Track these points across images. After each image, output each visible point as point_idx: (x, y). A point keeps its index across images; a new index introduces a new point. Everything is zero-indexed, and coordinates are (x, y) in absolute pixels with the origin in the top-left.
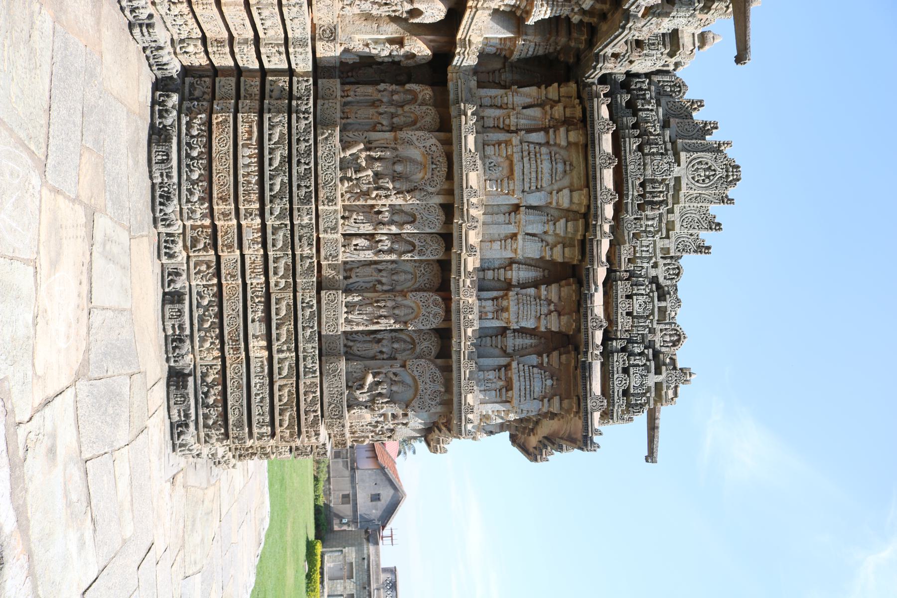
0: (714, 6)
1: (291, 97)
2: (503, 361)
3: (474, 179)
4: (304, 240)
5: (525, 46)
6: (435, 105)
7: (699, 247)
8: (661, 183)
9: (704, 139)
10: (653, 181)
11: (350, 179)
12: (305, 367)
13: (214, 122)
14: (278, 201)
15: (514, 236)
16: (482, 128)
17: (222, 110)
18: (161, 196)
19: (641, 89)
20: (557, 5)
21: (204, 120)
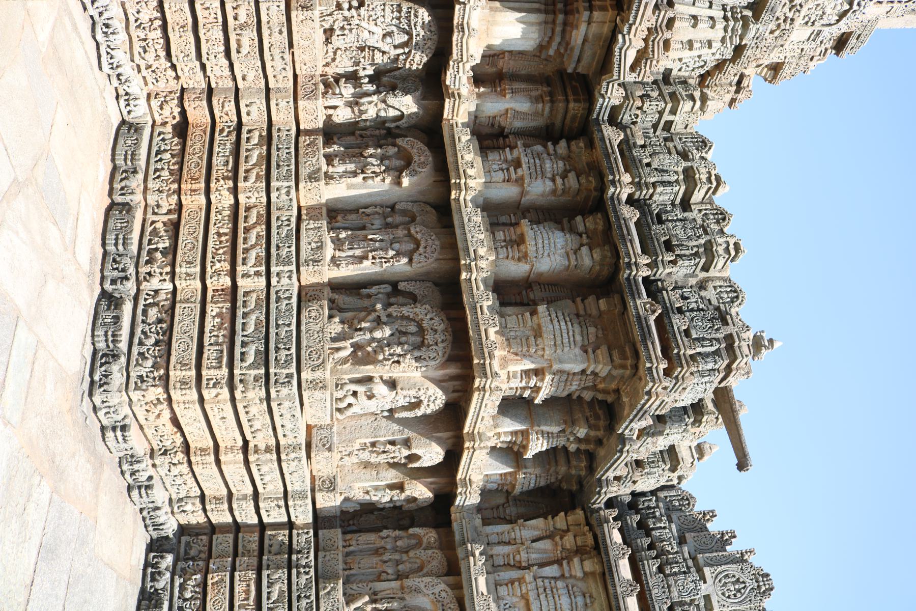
0: (704, 419)
1: (290, 551)
5: (526, 480)
6: (441, 548)
9: (725, 551)
13: (210, 582)
16: (493, 568)
17: (218, 570)
19: (649, 508)
20: (553, 437)
21: (199, 581)
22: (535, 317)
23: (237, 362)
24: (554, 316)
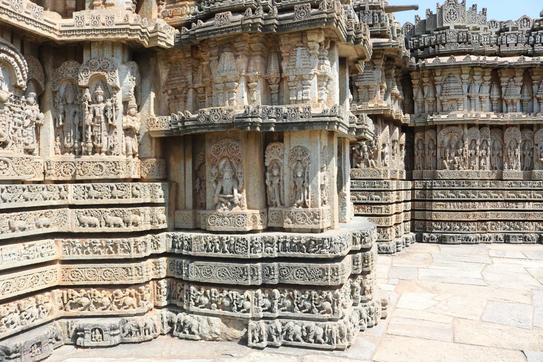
2: (535, 101)
3: (459, 115)
4: (484, 185)
6: (424, 131)
7: (483, 14)
8: (459, 35)
9: (436, 15)
10: (458, 38)
11: (459, 166)
12: (538, 187)
13: (436, 219)
14: (469, 195)
15: (480, 98)
16: (435, 111)
18: (467, 241)
19: (413, 44)
22: (360, 87)
23: (380, 202)
24: (360, 80)
